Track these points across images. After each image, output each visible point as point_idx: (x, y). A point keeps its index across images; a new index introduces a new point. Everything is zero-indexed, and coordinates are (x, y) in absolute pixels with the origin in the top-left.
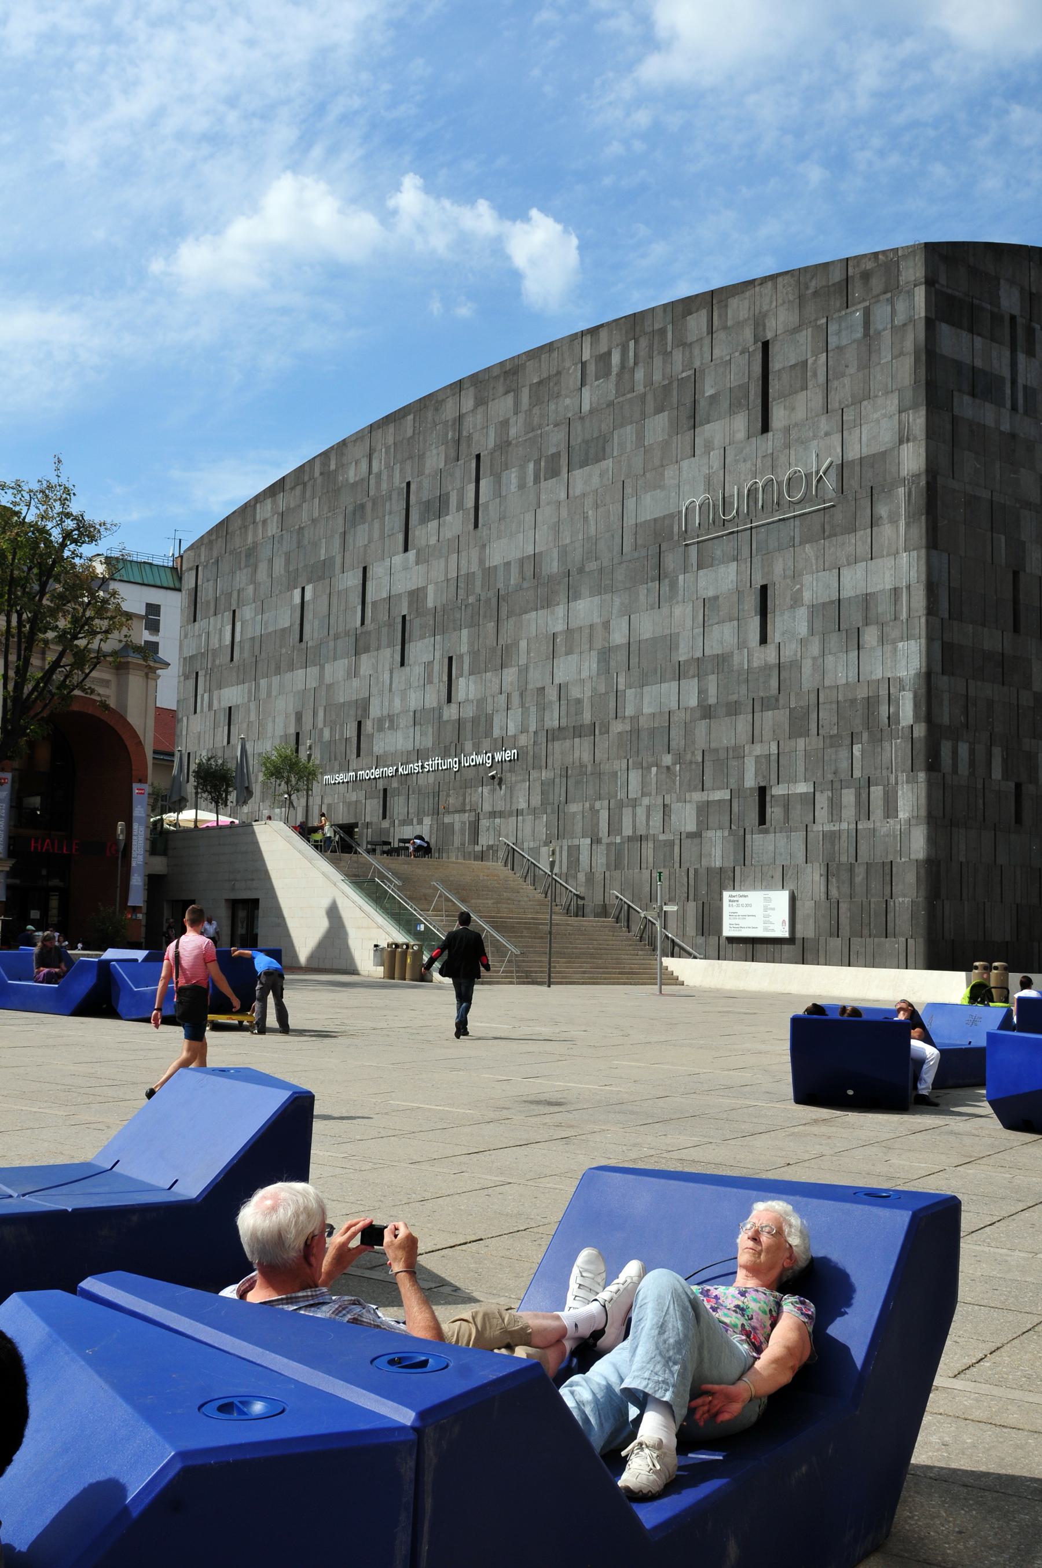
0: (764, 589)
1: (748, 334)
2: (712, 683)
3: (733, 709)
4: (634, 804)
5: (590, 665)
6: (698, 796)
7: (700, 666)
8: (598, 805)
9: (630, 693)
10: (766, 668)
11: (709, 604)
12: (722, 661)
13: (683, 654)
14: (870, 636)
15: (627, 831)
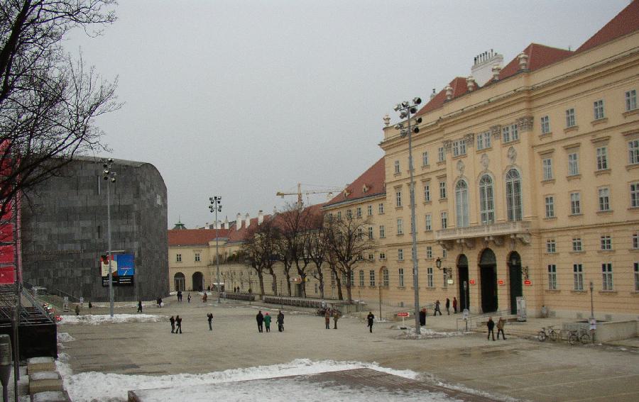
0: (99, 227)
1: (93, 173)
2: (85, 245)
3: (92, 251)
4: (61, 270)
5: (45, 238)
6: (81, 269)
7: (82, 241)
8: (49, 270)
9: (59, 245)
10: (100, 243)
11: (84, 228)
12: (88, 241)
13: (76, 238)
14: (127, 240)
15: (59, 275)
